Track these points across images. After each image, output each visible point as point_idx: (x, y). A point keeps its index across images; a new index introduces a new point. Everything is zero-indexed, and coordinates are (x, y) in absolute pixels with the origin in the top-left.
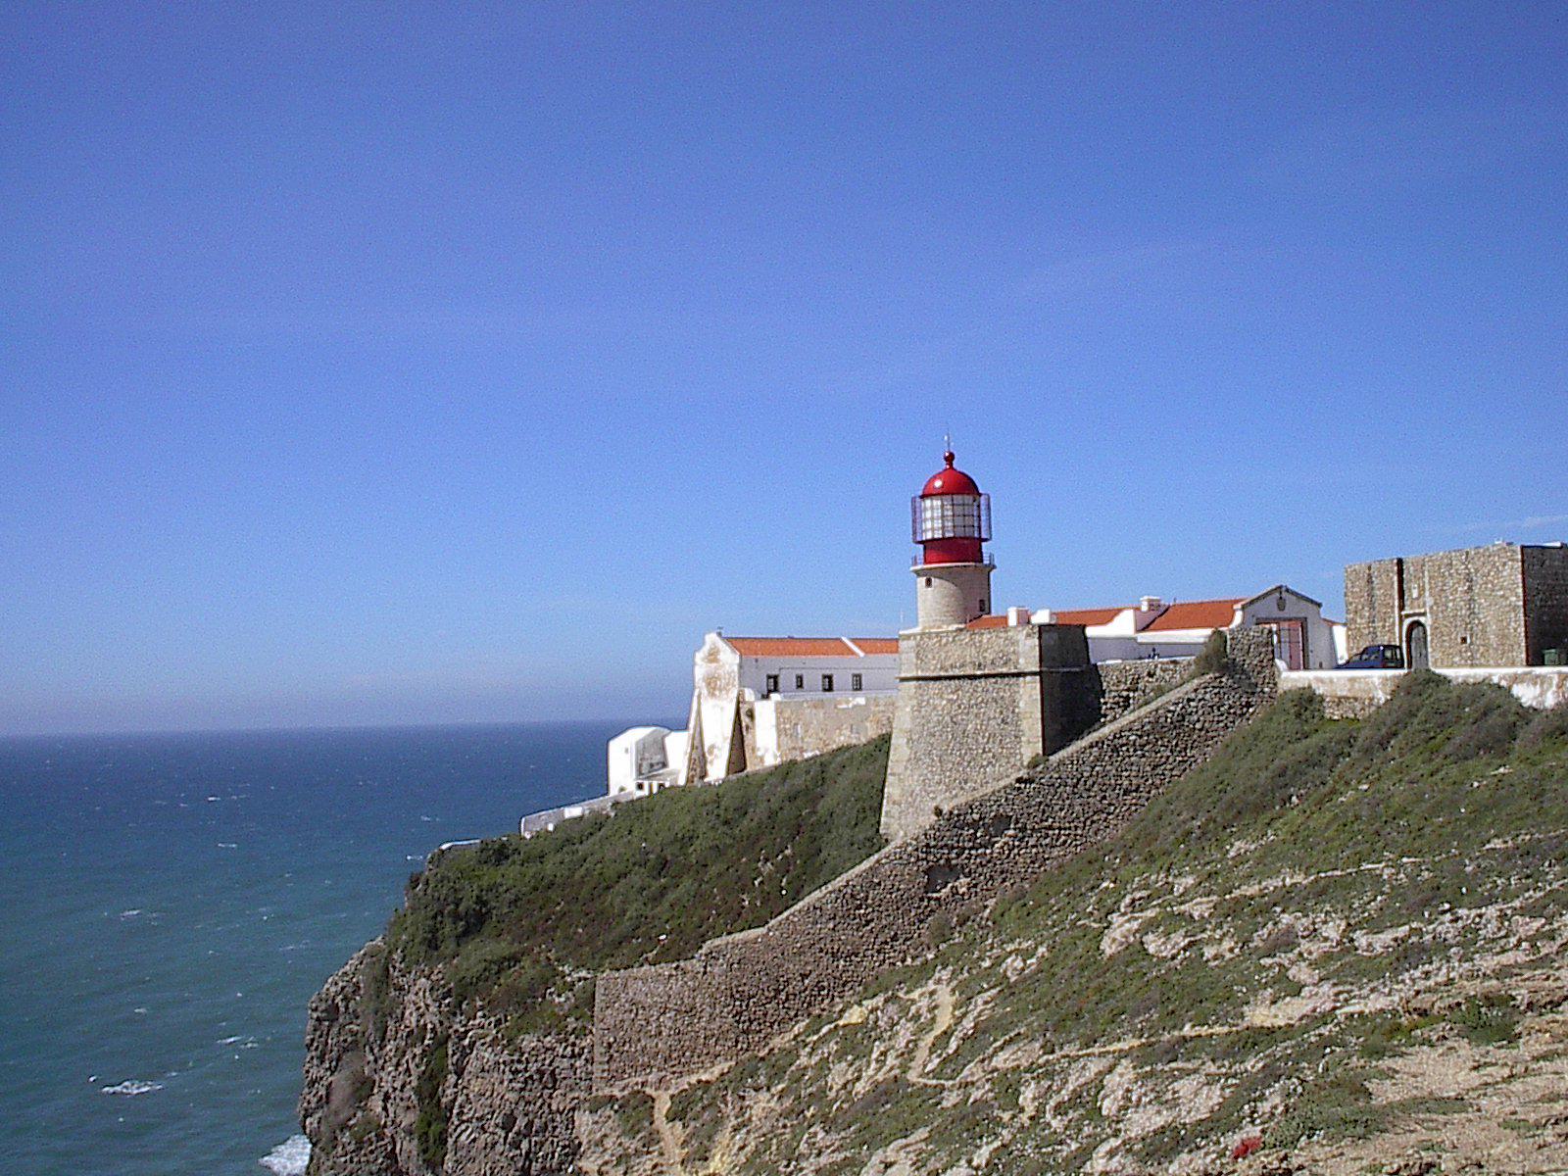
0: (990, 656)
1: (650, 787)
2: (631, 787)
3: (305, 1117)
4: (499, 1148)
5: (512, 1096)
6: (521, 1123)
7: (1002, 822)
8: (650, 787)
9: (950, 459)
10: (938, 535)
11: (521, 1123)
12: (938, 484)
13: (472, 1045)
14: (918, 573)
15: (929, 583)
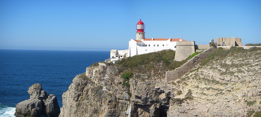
0: (188, 43)
1: (119, 57)
2: (115, 56)
3: (74, 98)
4: (144, 92)
5: (146, 86)
6: (147, 89)
7: (199, 57)
8: (119, 57)
9: (141, 20)
10: (141, 29)
11: (147, 89)
12: (139, 23)
13: (137, 82)
14: (137, 33)
15: (140, 34)
